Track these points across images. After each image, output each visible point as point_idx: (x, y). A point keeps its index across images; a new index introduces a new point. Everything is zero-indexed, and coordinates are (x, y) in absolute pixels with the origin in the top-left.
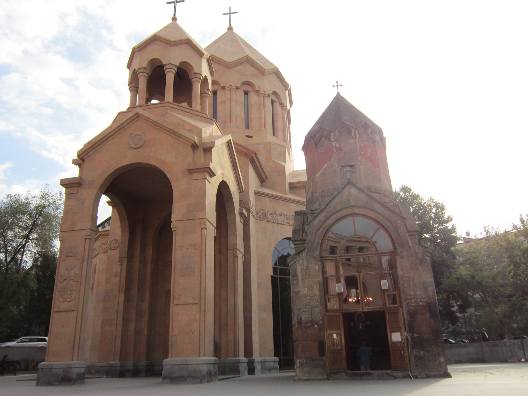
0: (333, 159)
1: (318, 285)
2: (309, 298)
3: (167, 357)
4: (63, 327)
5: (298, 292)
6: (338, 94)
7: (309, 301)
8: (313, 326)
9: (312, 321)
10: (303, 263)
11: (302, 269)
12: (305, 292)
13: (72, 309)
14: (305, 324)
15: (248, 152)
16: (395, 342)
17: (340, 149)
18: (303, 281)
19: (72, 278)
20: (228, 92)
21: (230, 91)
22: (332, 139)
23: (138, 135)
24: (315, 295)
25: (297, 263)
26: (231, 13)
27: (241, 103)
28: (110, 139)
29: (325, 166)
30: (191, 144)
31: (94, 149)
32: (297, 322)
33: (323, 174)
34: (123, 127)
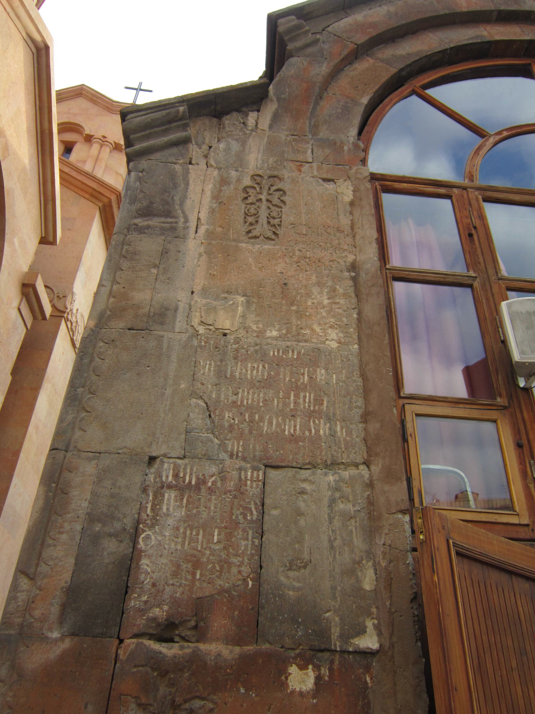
1: (345, 286)
2: (255, 370)
7: (247, 396)
8: (274, 669)
9: (254, 611)
10: (240, 162)
11: (224, 181)
12: (224, 322)
14: (166, 632)
15: (102, 190)
18: (220, 248)
20: (96, 147)
21: (102, 146)
24: (315, 357)
25: (194, 151)
26: (141, 90)
27: (117, 173)
32: (73, 594)
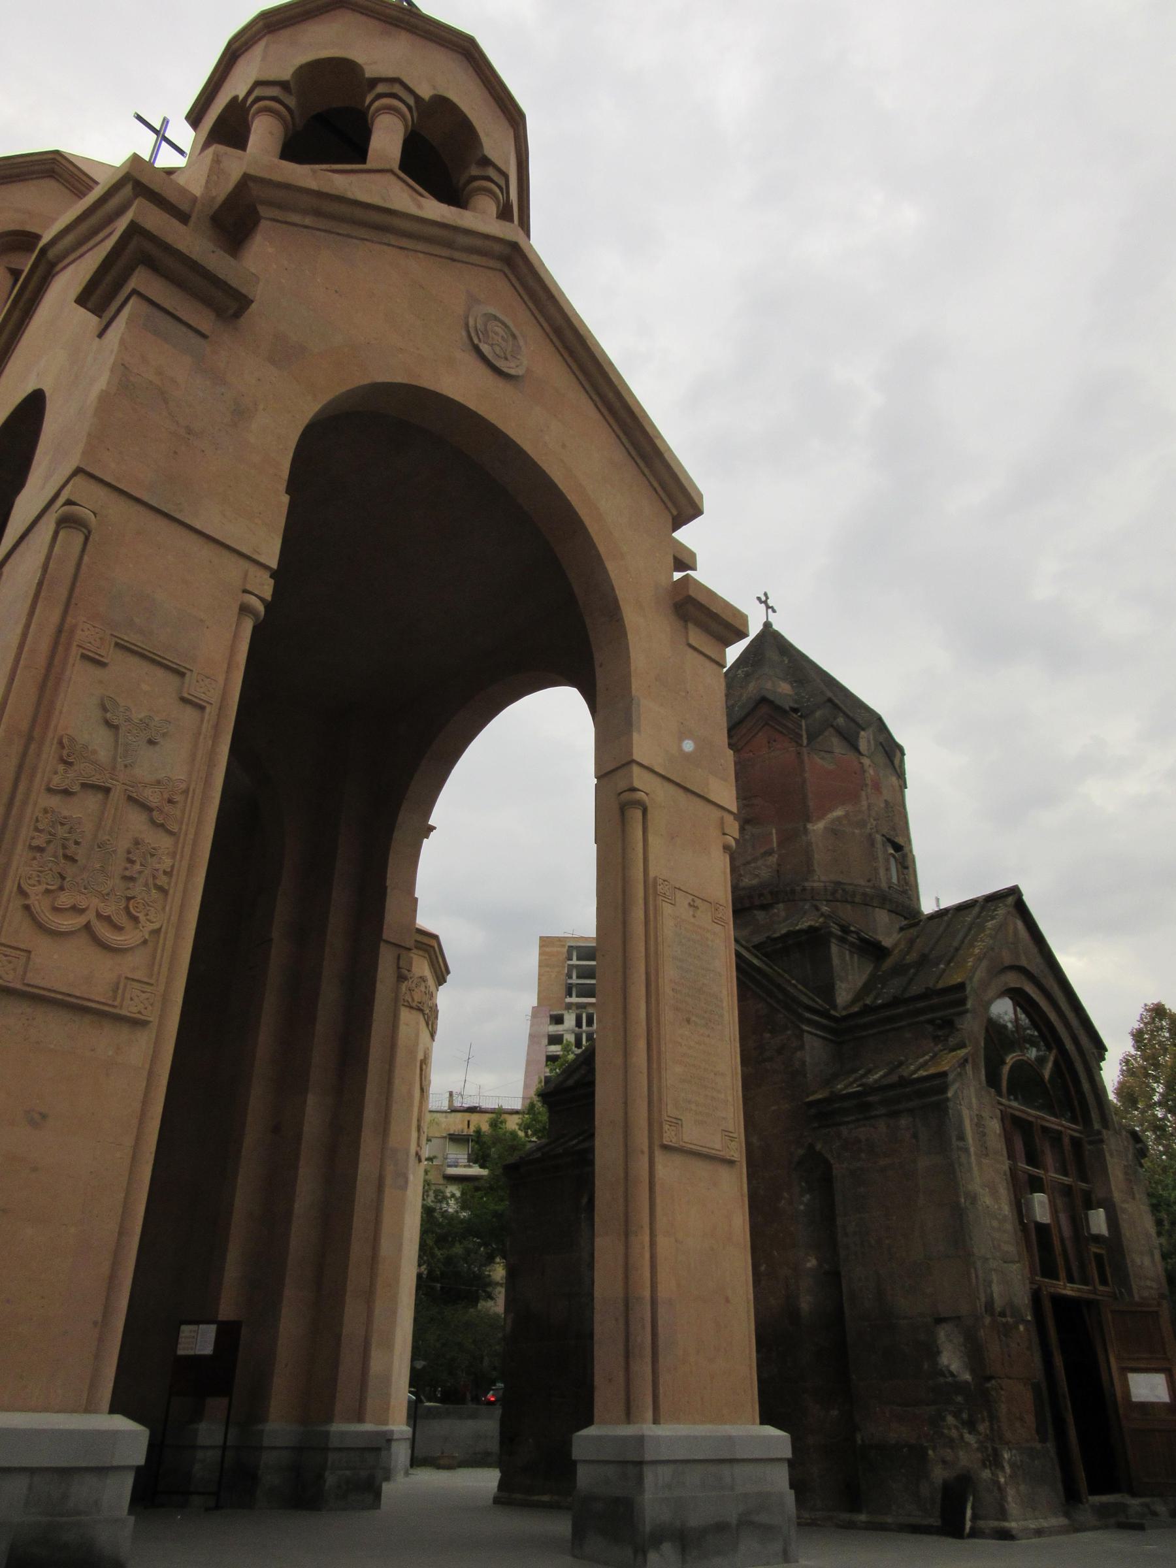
0: (864, 803)
3: (589, 1422)
4: (37, 1120)
5: (974, 1199)
6: (767, 625)
13: (129, 1009)
16: (1144, 1407)
17: (877, 787)
19: (152, 797)
22: (863, 746)
23: (503, 323)
28: (393, 240)
29: (839, 812)
30: (675, 513)
31: (318, 213)
33: (834, 832)
34: (450, 245)
